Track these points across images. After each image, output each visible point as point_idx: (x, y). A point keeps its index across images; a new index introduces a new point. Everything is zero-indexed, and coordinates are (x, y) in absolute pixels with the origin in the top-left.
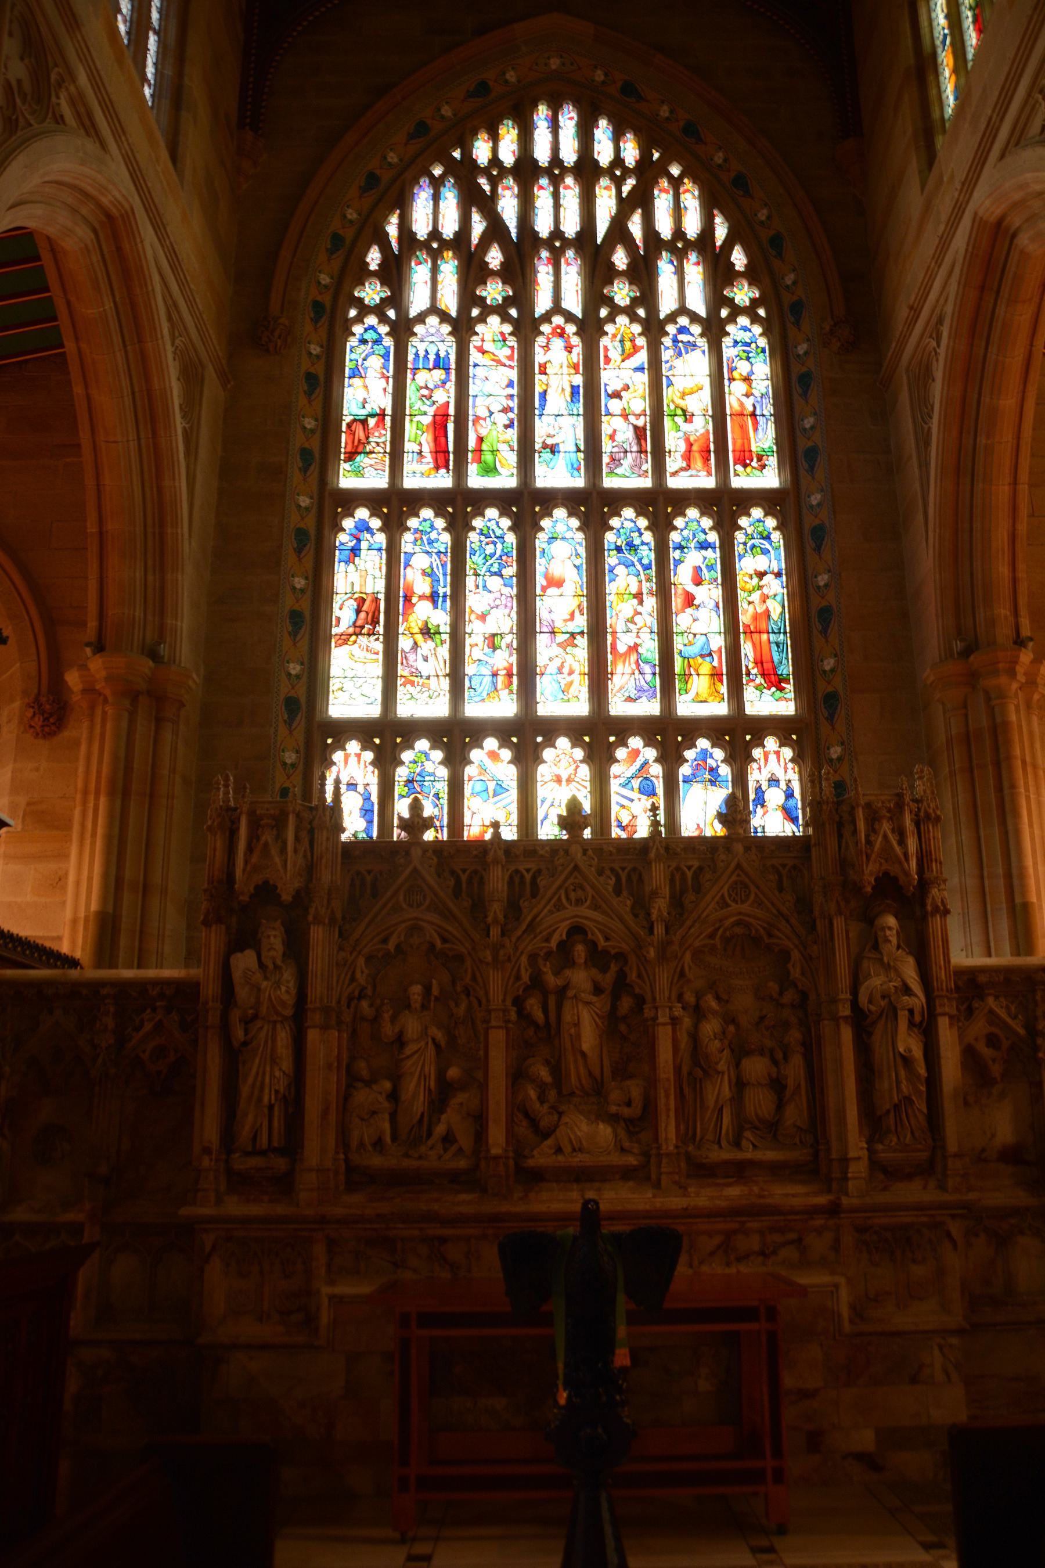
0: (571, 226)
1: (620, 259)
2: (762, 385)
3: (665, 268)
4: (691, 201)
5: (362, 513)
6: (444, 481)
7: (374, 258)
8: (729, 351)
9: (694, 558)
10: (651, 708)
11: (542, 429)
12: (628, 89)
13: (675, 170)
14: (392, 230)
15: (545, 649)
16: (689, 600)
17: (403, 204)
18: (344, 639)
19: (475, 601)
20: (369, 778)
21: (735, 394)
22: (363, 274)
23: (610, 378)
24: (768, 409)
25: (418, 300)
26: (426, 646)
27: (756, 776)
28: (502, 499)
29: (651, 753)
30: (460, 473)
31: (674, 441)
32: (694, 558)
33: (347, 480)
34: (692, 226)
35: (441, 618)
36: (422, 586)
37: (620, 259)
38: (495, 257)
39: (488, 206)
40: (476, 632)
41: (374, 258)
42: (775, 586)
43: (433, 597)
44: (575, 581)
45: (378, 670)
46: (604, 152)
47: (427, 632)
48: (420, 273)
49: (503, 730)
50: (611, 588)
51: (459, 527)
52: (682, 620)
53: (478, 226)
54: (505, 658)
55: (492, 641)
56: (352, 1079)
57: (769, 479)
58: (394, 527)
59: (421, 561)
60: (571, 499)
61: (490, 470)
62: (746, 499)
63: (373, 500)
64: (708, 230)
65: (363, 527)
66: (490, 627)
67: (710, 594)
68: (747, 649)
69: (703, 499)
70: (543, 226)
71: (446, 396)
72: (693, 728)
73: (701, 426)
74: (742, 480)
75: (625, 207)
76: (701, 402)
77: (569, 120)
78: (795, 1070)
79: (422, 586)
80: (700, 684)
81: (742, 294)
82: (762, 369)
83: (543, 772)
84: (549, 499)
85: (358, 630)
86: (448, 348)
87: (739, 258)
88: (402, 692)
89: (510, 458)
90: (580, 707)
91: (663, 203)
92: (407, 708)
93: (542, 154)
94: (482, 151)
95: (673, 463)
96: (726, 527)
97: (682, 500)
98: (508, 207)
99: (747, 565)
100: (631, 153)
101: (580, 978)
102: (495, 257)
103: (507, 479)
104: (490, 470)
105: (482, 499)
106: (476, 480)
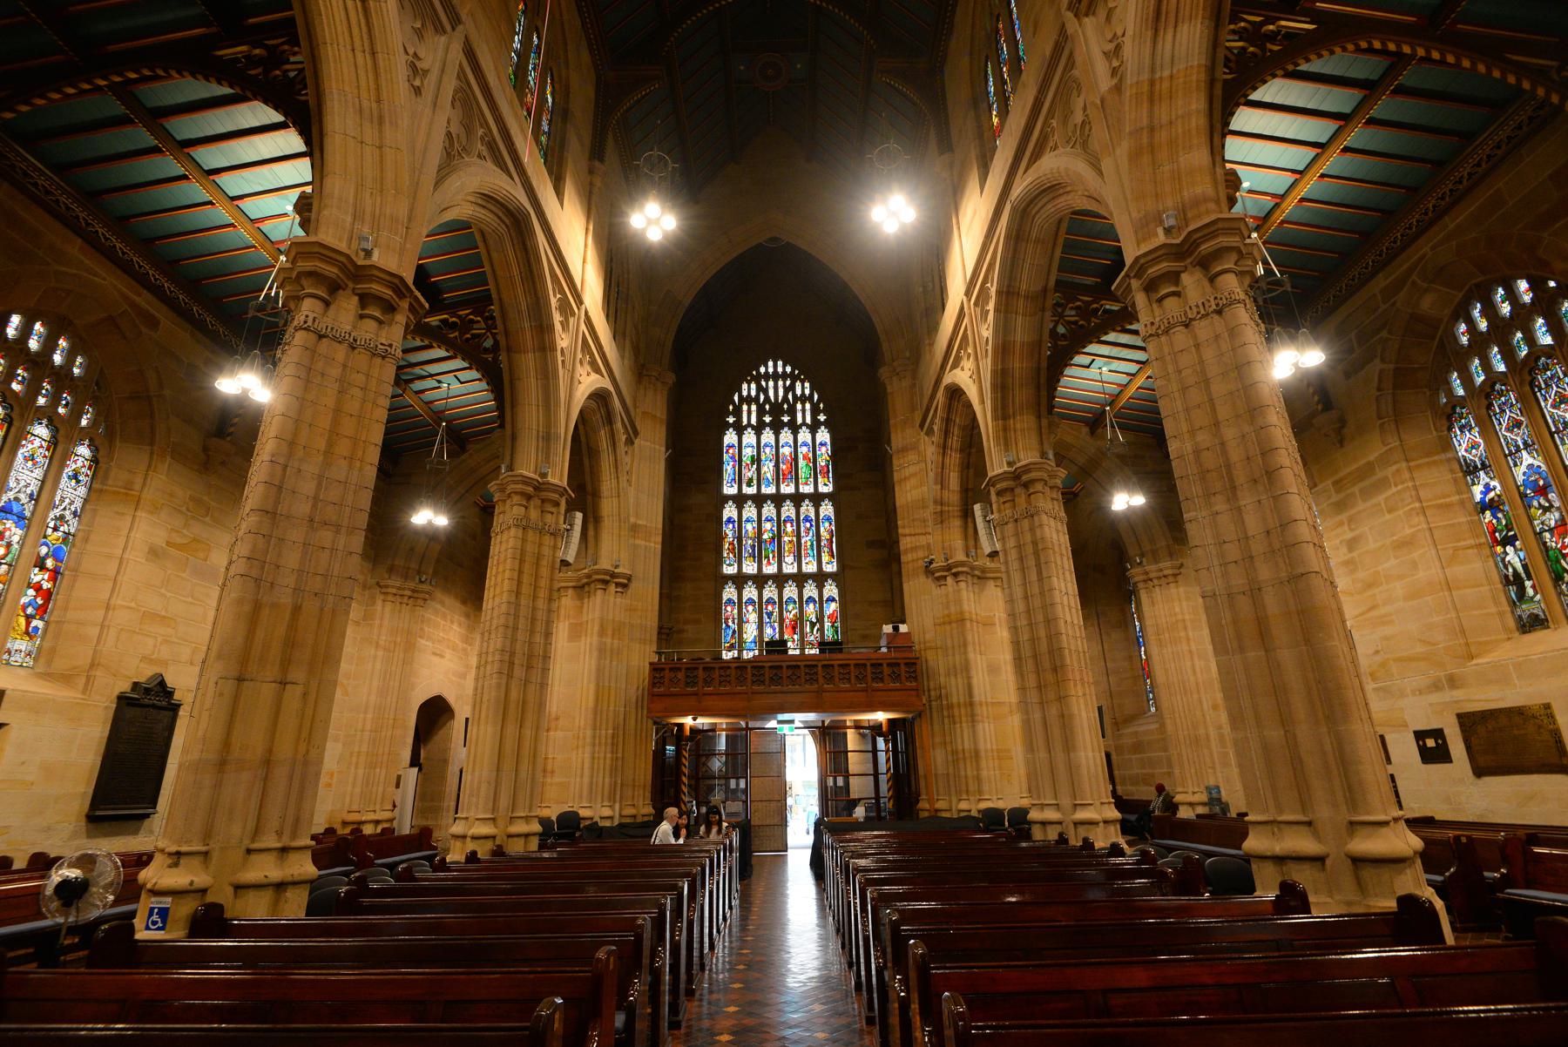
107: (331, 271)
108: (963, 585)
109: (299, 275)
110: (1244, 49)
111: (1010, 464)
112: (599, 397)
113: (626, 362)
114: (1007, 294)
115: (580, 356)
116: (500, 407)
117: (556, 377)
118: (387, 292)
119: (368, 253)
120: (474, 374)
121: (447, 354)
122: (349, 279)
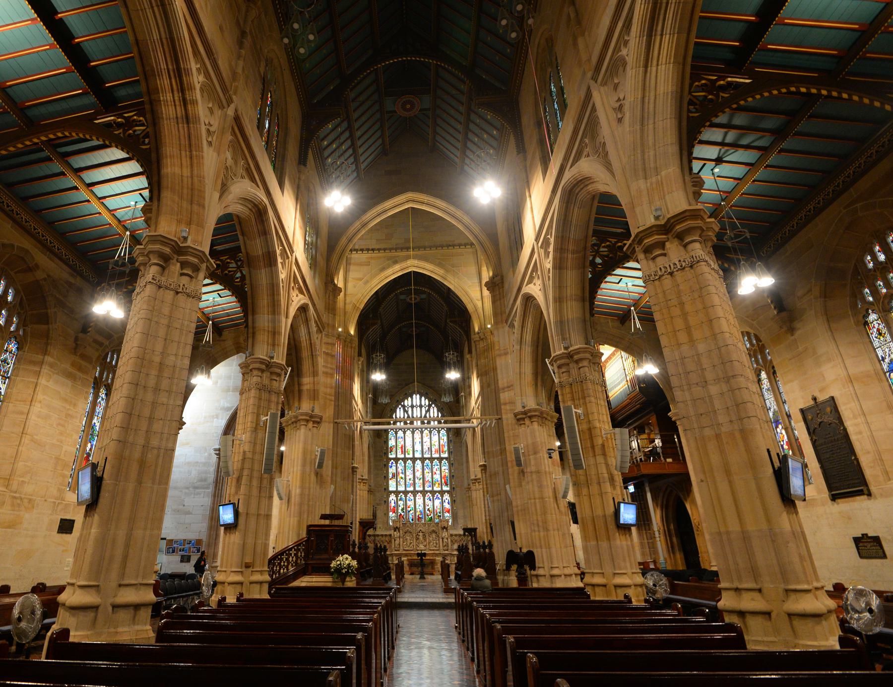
2: (446, 440)
6: (402, 456)
8: (441, 435)
9: (436, 467)
10: (430, 489)
12: (426, 393)
14: (394, 416)
15: (417, 481)
17: (396, 412)
19: (407, 473)
20: (395, 499)
21: (442, 442)
23: (424, 440)
27: (444, 498)
28: (410, 459)
31: (433, 450)
32: (436, 467)
34: (436, 416)
35: (403, 476)
39: (407, 412)
40: (408, 478)
42: (447, 471)
44: (420, 471)
46: (423, 404)
47: (402, 478)
49: (411, 492)
51: (405, 463)
52: (434, 476)
53: (406, 416)
54: (411, 482)
57: (446, 455)
58: (396, 463)
60: (420, 459)
62: (443, 459)
63: (393, 459)
64: (438, 416)
67: (438, 472)
69: (437, 459)
70: (415, 416)
71: (403, 443)
72: (436, 492)
73: (437, 447)
74: (443, 455)
75: (426, 412)
76: (437, 444)
77: (418, 396)
80: (437, 485)
82: (445, 438)
84: (417, 459)
86: (403, 435)
89: (411, 453)
90: (421, 489)
92: (399, 489)
93: (415, 404)
94: (406, 404)
95: (433, 453)
96: (440, 463)
97: (434, 459)
99: (443, 468)
100: (427, 404)
101: (421, 534)
103: (411, 456)
105: (408, 459)
106: (407, 456)
107: (167, 250)
108: (535, 424)
109: (150, 252)
110: (705, 97)
111: (566, 348)
112: (303, 309)
113: (317, 281)
114: (560, 250)
115: (292, 285)
116: (246, 316)
117: (279, 294)
118: (195, 260)
119: (185, 239)
120: (227, 292)
121: (211, 282)
122: (175, 253)
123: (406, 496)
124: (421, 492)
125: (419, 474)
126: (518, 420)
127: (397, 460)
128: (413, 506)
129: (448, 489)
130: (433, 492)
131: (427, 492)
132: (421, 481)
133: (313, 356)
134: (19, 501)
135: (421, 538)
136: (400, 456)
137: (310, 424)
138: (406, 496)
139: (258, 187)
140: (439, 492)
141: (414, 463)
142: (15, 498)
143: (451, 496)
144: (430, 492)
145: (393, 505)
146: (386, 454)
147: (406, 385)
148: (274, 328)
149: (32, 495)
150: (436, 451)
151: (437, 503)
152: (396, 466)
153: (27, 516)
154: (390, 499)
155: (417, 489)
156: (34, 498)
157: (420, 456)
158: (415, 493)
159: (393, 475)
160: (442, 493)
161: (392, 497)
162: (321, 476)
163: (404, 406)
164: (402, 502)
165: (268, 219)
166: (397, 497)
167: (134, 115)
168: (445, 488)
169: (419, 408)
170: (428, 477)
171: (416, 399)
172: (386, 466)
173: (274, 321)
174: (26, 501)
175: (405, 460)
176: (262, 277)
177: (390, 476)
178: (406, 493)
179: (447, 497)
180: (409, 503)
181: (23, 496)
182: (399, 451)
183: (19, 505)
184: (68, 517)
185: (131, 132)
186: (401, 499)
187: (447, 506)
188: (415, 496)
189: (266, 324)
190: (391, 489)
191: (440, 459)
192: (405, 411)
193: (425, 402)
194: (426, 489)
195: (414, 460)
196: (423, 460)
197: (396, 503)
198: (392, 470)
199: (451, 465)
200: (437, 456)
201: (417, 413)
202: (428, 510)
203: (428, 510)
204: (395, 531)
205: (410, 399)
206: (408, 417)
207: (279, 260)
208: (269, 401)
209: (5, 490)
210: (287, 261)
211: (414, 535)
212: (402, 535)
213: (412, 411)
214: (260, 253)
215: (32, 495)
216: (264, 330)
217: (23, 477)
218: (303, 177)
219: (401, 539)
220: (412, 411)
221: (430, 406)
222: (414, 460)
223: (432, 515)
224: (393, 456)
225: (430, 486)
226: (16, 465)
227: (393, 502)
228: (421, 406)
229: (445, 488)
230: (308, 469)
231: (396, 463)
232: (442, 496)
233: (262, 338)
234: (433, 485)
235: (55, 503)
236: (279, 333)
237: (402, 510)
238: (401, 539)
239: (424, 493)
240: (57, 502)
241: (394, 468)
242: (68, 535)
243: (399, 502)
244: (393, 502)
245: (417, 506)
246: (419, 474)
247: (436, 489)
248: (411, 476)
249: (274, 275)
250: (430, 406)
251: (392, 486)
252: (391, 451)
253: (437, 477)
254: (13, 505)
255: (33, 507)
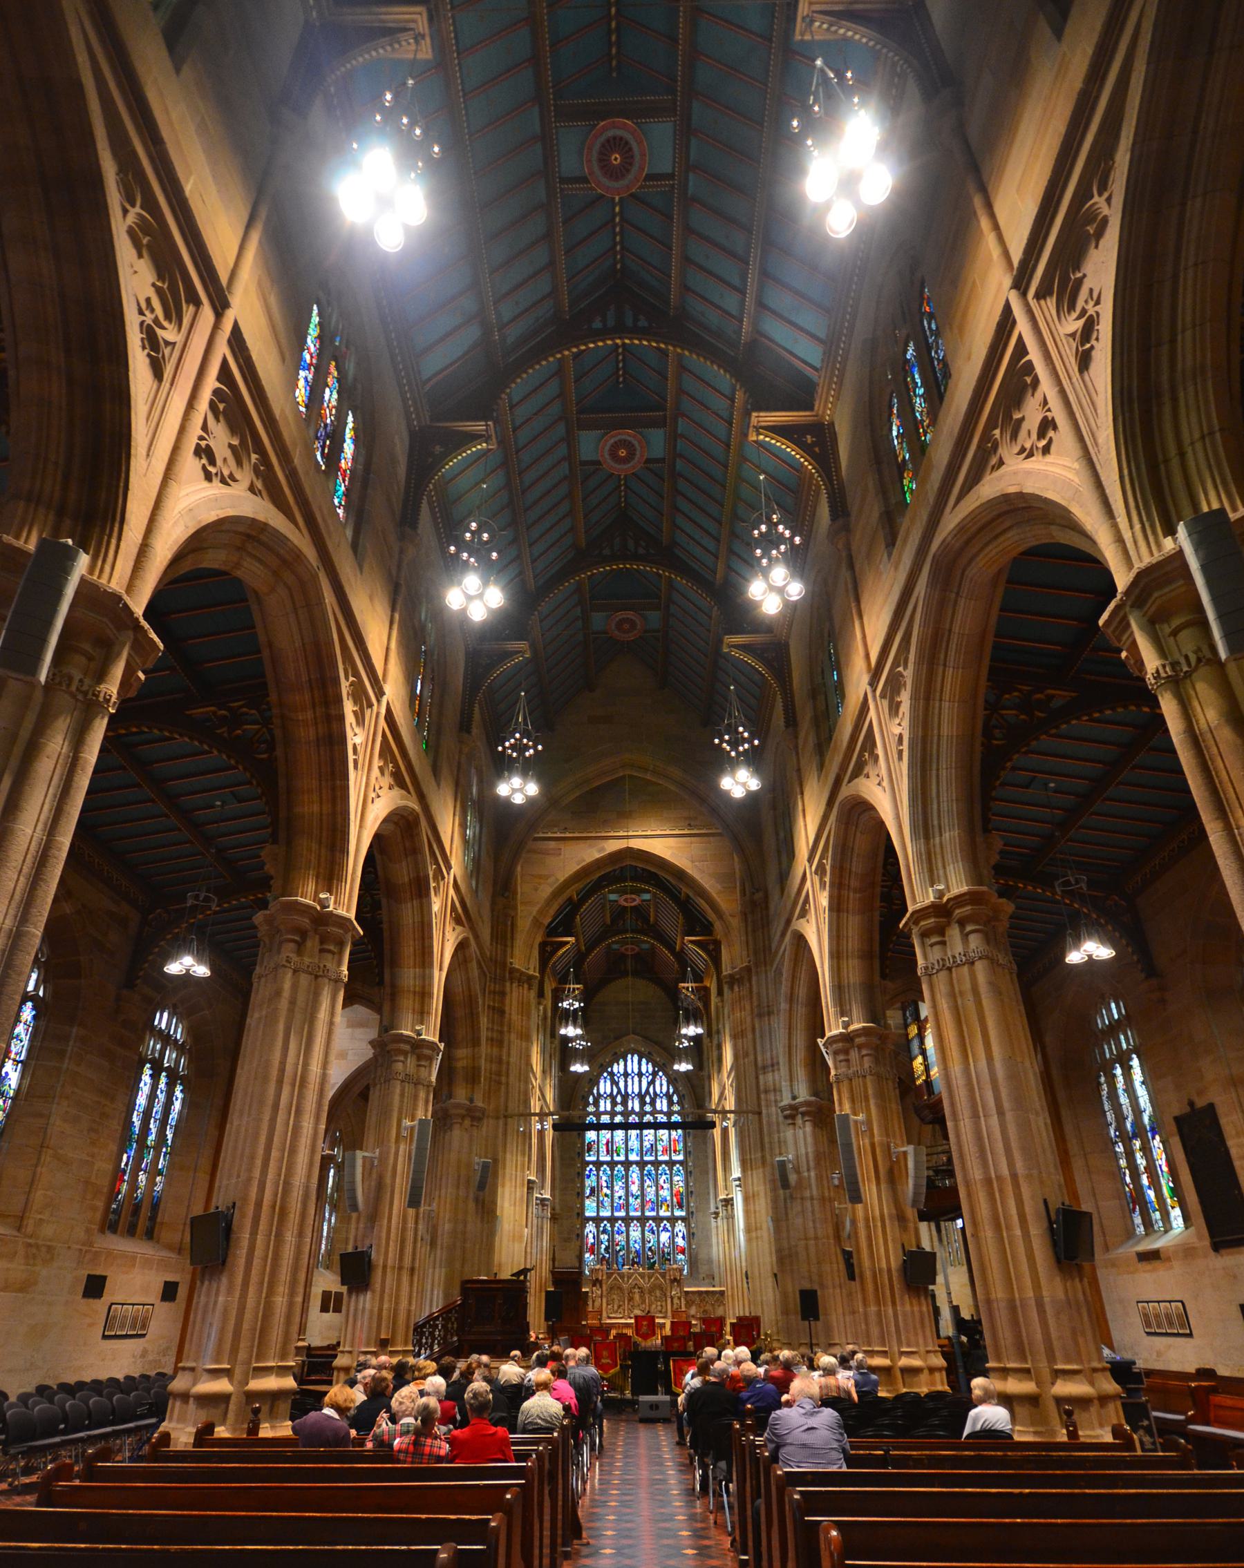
0: (636, 1091)
1: (648, 1099)
3: (658, 1101)
4: (665, 1083)
5: (591, 1166)
6: (608, 1158)
7: (591, 1100)
9: (664, 1177)
10: (653, 1214)
11: (630, 1144)
12: (649, 1053)
13: (661, 1074)
14: (595, 1091)
15: (631, 1200)
16: (662, 1187)
17: (598, 1084)
18: (588, 1197)
19: (616, 1188)
22: (589, 1104)
24: (681, 1139)
25: (602, 1109)
26: (606, 1199)
27: (677, 1230)
29: (654, 1224)
30: (612, 1156)
31: (660, 1148)
33: (588, 1159)
34: (664, 1090)
36: (604, 1184)
37: (648, 1099)
38: (619, 1099)
39: (617, 1084)
40: (616, 1195)
41: (591, 1100)
43: (607, 1187)
45: (595, 1204)
46: (644, 1070)
47: (606, 1195)
48: (602, 1103)
49: (622, 1219)
50: (646, 1185)
51: (612, 1170)
52: (661, 1192)
55: (620, 1198)
56: (608, 1304)
57: (680, 1157)
58: (598, 1170)
59: (604, 1178)
60: (637, 1163)
61: (618, 1155)
65: (591, 1170)
66: (619, 1194)
67: (666, 1186)
68: (675, 1200)
70: (630, 1091)
72: (662, 1219)
73: (665, 1143)
74: (676, 1158)
75: (649, 1084)
77: (636, 1058)
78: (664, 1304)
79: (604, 1184)
80: (664, 1207)
81: (676, 1108)
83: (631, 1229)
84: (631, 1163)
85: (591, 1195)
87: (675, 1098)
88: (601, 1209)
89: (623, 1152)
90: (639, 1214)
91: (658, 1083)
92: (602, 1214)
93: (629, 1071)
94: (615, 1070)
95: (660, 1153)
96: (671, 1170)
98: (622, 1085)
99: (676, 1178)
100: (650, 1070)
101: (636, 1290)
102: (619, 1099)
103: (622, 1158)
104: (618, 1155)
106: (616, 1158)
123: (613, 1226)
124: (638, 1219)
125: (634, 1189)
126: (786, 1117)
127: (598, 1164)
128: (623, 1243)
129: (683, 1214)
130: (658, 1220)
131: (648, 1218)
132: (639, 1200)
133: (473, 1017)
134: (34, 1251)
135: (637, 1297)
136: (605, 1158)
137: (467, 1122)
138: (613, 1226)
139: (409, 793)
140: (668, 1219)
141: (627, 1170)
142: (30, 1245)
143: (688, 1226)
144: (653, 1219)
145: (591, 1240)
146: (581, 1155)
147: (617, 1038)
148: (424, 987)
149: (50, 1240)
150: (665, 1151)
151: (665, 1237)
152: (598, 1175)
153: (44, 1272)
154: (587, 1230)
155: (632, 1214)
156: (54, 1244)
157: (638, 1159)
158: (627, 1220)
159: (592, 1190)
160: (673, 1220)
161: (590, 1228)
162: (483, 1202)
163: (612, 1074)
164: (606, 1237)
165: (419, 834)
166: (597, 1227)
167: (241, 707)
168: (678, 1213)
169: (636, 1079)
170: (651, 1193)
171: (633, 1063)
172: (581, 1176)
173: (423, 977)
174: (44, 1249)
175: (612, 1164)
176: (408, 914)
177: (588, 1192)
178: (612, 1220)
179: (680, 1227)
180: (618, 1238)
181: (40, 1242)
182: (603, 1149)
183: (34, 1257)
184: (98, 1272)
185: (239, 732)
186: (605, 1231)
187: (680, 1242)
188: (628, 1227)
189: (412, 982)
190: (588, 1214)
191: (671, 1164)
192: (614, 1083)
193: (647, 1067)
194: (647, 1214)
195: (627, 1164)
196: (642, 1164)
197: (596, 1237)
198: (590, 1182)
199: (688, 1173)
200: (666, 1158)
201: (634, 1087)
202: (650, 1249)
203: (650, 1249)
204: (594, 1285)
205: (622, 1063)
206: (619, 1092)
207: (433, 885)
208: (416, 1097)
209: (17, 1234)
210: (442, 883)
211: (626, 1292)
212: (604, 1293)
213: (626, 1082)
214: (406, 879)
215: (50, 1240)
216: (409, 991)
217: (40, 1213)
218: (466, 750)
219: (604, 1300)
220: (626, 1082)
221: (655, 1074)
222: (627, 1164)
223: (656, 1258)
224: (594, 1158)
225: (653, 1210)
226: (32, 1195)
227: (591, 1236)
228: (640, 1075)
229: (678, 1213)
230: (462, 1193)
231: (598, 1170)
232: (673, 1226)
233: (407, 1004)
234: (658, 1204)
235: (81, 1250)
236: (430, 995)
237: (607, 1249)
238: (604, 1300)
239: (643, 1220)
240: (84, 1248)
241: (593, 1178)
242: (97, 1301)
243: (602, 1237)
244: (591, 1236)
245: (631, 1242)
246: (634, 1189)
247: (662, 1213)
248: (622, 1193)
249: (425, 909)
250: (655, 1074)
251: (590, 1209)
252: (589, 1150)
253: (665, 1193)
254: (27, 1257)
255: (52, 1259)
